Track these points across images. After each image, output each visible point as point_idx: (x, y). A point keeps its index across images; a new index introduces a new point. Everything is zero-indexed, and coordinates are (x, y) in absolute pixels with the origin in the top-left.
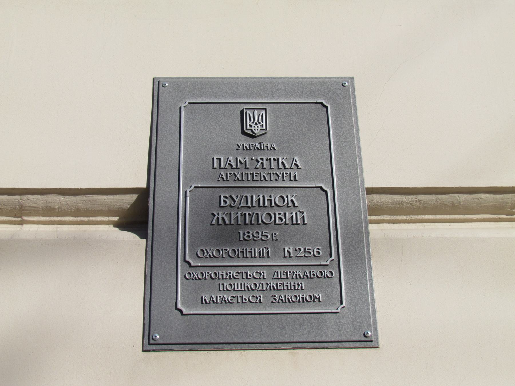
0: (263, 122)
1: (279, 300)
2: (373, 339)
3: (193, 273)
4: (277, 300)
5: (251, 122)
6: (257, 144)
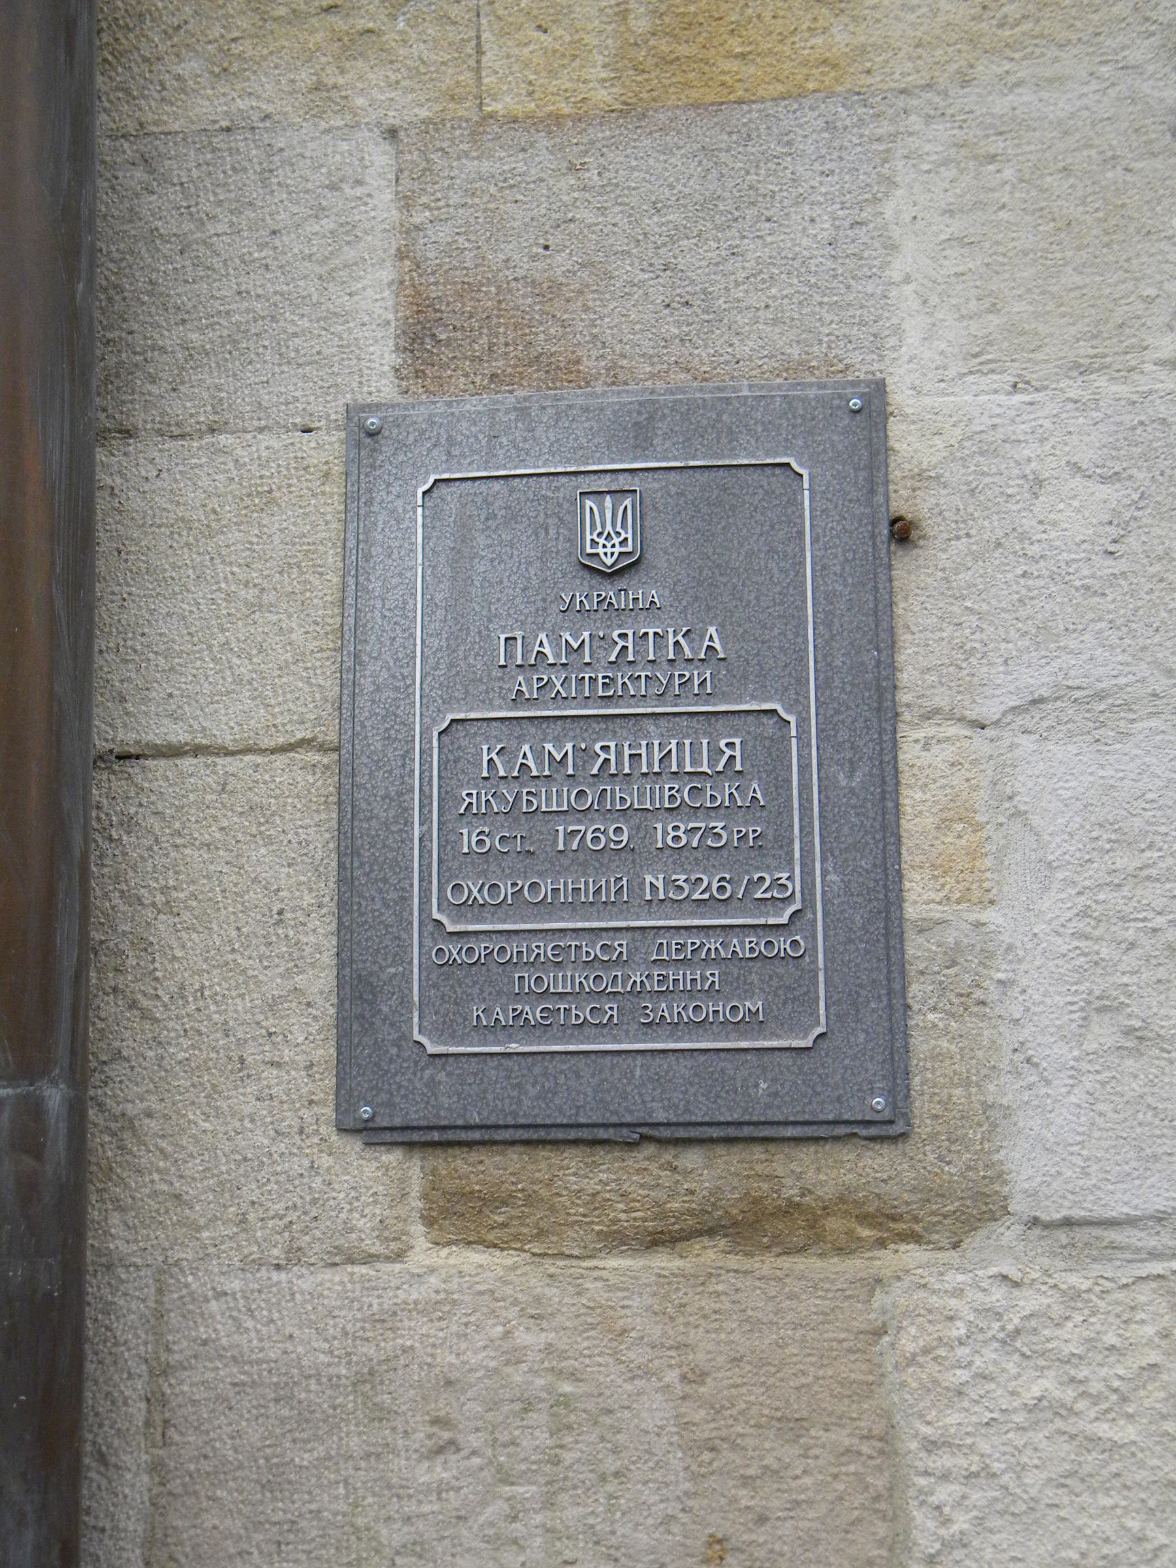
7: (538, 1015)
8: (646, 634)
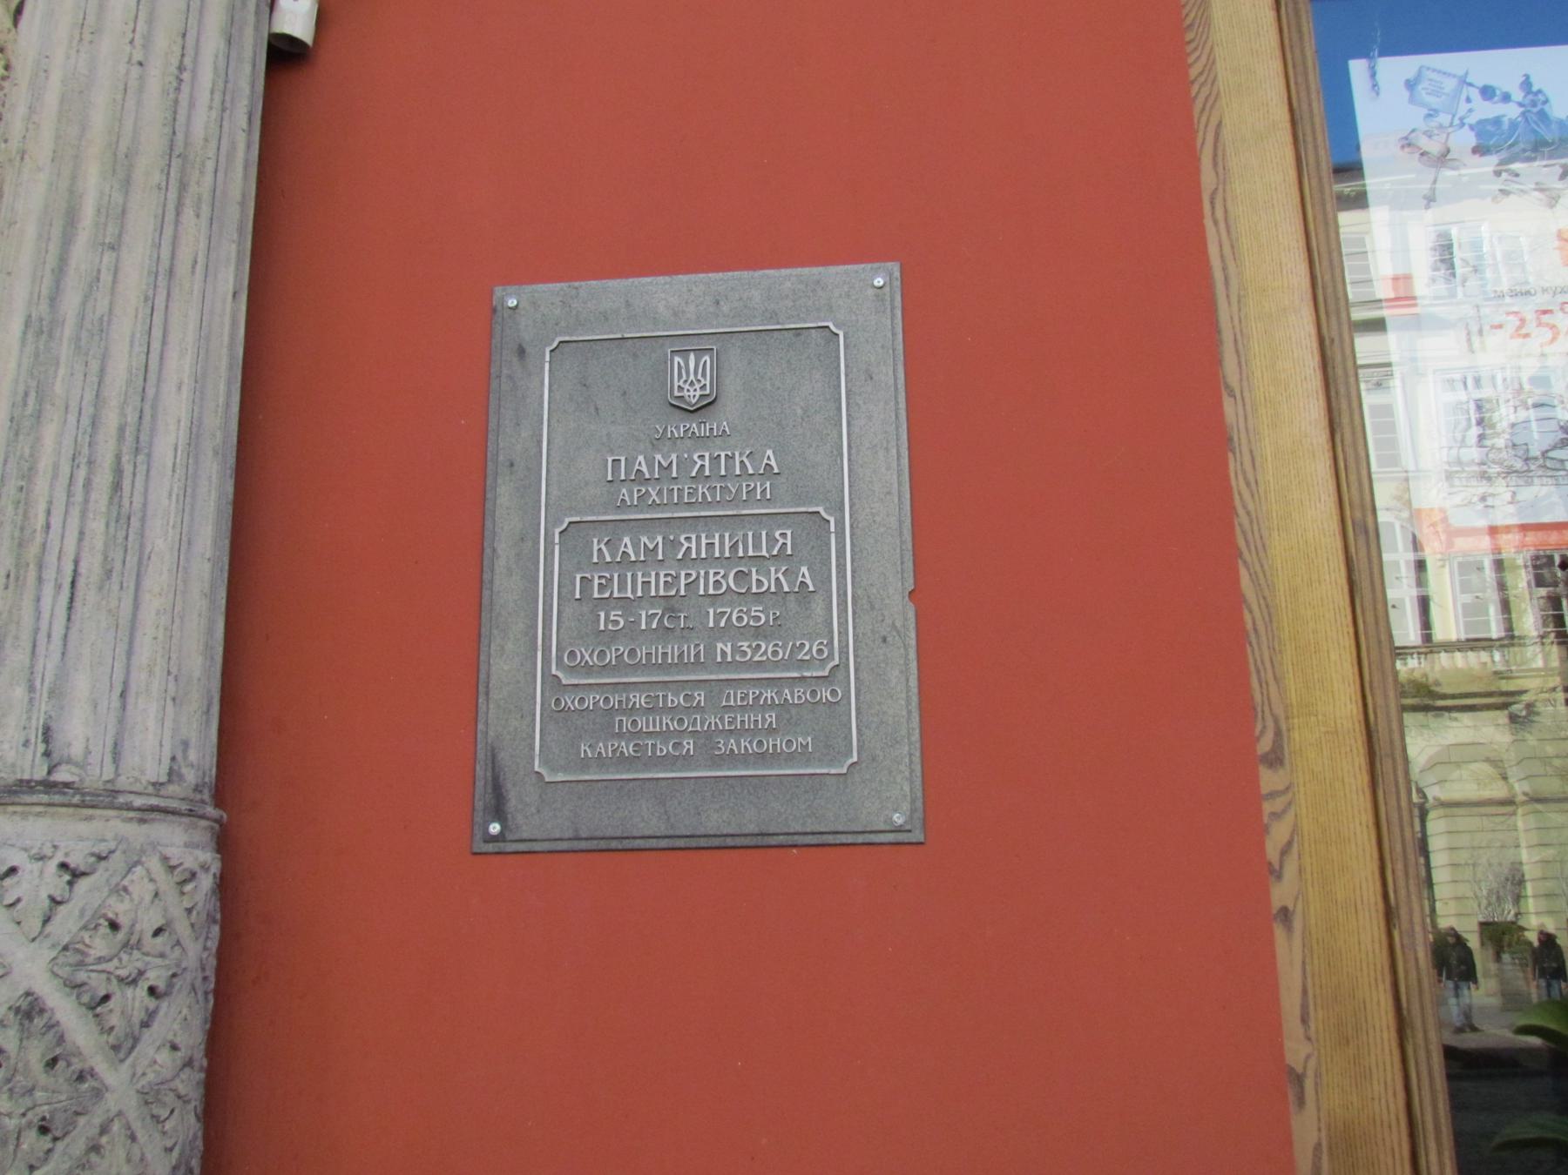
5: (682, 381)
6: (694, 425)
7: (631, 749)
8: (719, 456)
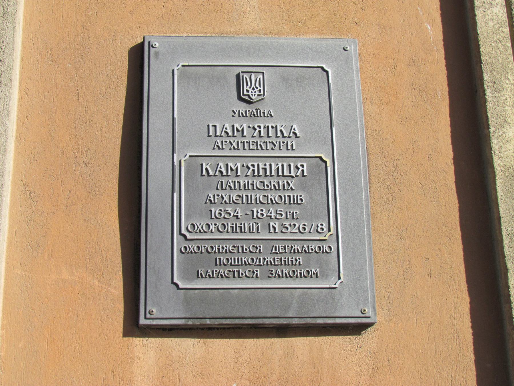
0: (260, 87)
1: (276, 275)
2: (371, 316)
3: (189, 246)
4: (274, 274)
5: (248, 87)
6: (254, 110)
